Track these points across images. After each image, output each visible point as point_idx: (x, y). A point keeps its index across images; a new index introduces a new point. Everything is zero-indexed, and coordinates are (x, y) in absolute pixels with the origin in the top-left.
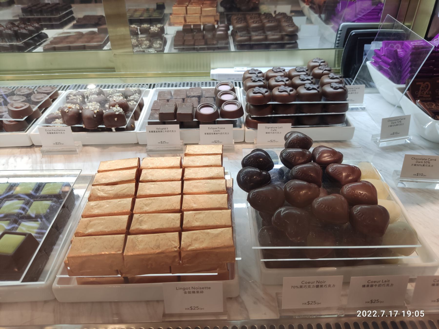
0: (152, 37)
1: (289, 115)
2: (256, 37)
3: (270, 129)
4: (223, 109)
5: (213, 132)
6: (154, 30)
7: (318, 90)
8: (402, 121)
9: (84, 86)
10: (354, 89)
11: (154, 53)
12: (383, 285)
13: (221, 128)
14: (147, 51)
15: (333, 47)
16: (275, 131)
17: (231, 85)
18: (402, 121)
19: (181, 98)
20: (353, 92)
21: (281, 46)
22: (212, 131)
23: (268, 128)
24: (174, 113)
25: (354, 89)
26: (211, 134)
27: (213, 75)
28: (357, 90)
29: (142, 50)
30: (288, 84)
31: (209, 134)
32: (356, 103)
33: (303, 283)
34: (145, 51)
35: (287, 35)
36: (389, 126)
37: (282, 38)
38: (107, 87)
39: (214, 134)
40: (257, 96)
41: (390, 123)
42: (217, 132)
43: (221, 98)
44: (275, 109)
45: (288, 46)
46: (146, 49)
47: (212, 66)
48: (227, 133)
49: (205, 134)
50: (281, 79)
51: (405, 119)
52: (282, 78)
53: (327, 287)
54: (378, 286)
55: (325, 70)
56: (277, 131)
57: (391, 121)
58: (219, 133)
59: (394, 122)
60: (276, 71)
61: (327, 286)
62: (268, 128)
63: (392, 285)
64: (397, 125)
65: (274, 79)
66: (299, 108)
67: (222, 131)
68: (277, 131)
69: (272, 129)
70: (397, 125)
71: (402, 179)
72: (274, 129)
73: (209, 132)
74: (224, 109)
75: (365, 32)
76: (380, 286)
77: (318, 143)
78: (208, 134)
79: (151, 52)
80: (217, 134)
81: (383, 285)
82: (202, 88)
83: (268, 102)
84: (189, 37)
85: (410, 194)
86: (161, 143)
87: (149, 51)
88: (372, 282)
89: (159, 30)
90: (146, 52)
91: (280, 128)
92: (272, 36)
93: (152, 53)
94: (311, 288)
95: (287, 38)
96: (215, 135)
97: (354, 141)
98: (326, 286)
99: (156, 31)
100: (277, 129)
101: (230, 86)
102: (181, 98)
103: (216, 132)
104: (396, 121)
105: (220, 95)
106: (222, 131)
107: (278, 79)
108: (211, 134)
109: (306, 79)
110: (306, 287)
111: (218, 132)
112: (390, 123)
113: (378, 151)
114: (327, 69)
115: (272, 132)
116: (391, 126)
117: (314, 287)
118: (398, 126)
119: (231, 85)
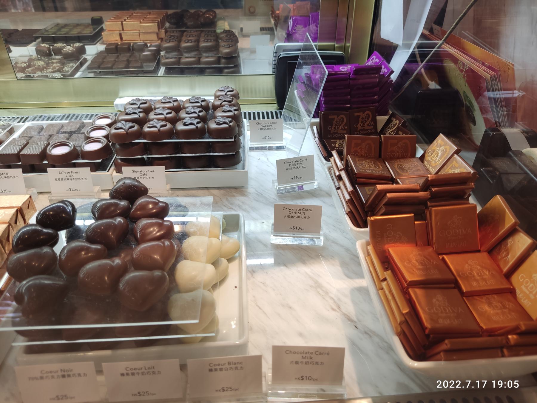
0: (65, 58)
1: (198, 155)
2: (188, 58)
3: (139, 173)
4: (83, 150)
5: (66, 178)
6: (68, 50)
7: (231, 124)
8: (303, 162)
9: (65, 116)
10: (270, 124)
11: (59, 77)
12: (231, 369)
13: (75, 173)
14: (51, 76)
15: (271, 73)
16: (145, 176)
17: (112, 117)
18: (303, 162)
19: (47, 135)
20: (269, 127)
21: (219, 71)
22: (63, 176)
23: (136, 172)
24: (39, 154)
25: (270, 124)
26: (63, 179)
27: (117, 105)
28: (274, 126)
29: (45, 74)
30: (201, 116)
31: (61, 179)
32: (274, 140)
33: (211, 365)
34: (49, 76)
35: (224, 58)
36: (287, 169)
37: (218, 61)
38: (50, 119)
39: (68, 179)
40: (155, 131)
41: (288, 166)
42: (70, 178)
43: (89, 135)
44: (146, 148)
45: (226, 70)
46: (50, 74)
47: (121, 94)
48: (151, 178)
49: (56, 180)
50: (192, 110)
51: (306, 160)
52: (194, 109)
53: (314, 364)
54: (304, 364)
55: (225, 101)
56: (148, 176)
57: (289, 163)
58: (74, 179)
59: (292, 164)
60: (192, 101)
61: (313, 363)
62: (136, 172)
63: (242, 368)
64: (297, 167)
65: (185, 111)
66: (178, 148)
67: (77, 176)
68: (148, 176)
69: (141, 173)
70: (297, 167)
71: (277, 233)
72: (144, 173)
73: (60, 178)
74: (84, 149)
75: (336, 55)
76: (308, 363)
77: (208, 189)
78: (59, 180)
79: (56, 76)
80: (71, 179)
81: (311, 362)
82: (84, 121)
83: (135, 140)
84: (112, 58)
85: (282, 251)
86: (69, 190)
87: (53, 75)
88: (131, 369)
89: (74, 50)
90: (49, 77)
91: (151, 172)
92: (207, 58)
93: (57, 78)
94: (319, 365)
95: (223, 61)
96: (69, 181)
97: (252, 187)
98: (232, 368)
99: (70, 52)
100: (148, 173)
101: (111, 119)
102: (48, 134)
103: (69, 178)
104: (296, 163)
105: (88, 132)
106: (77, 176)
107: (188, 111)
108: (63, 179)
109: (193, 112)
110: (313, 364)
111: (72, 178)
112: (288, 166)
113: (274, 199)
114: (226, 99)
115: (142, 177)
116: (289, 169)
117: (322, 364)
118: (299, 169)
119: (112, 117)
